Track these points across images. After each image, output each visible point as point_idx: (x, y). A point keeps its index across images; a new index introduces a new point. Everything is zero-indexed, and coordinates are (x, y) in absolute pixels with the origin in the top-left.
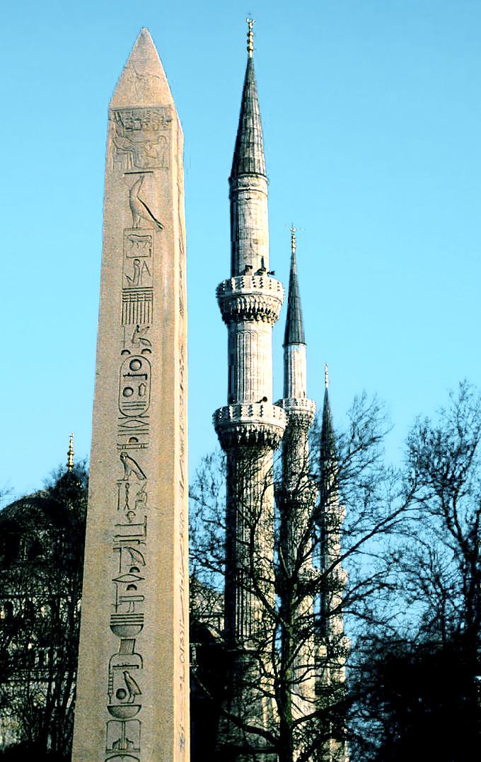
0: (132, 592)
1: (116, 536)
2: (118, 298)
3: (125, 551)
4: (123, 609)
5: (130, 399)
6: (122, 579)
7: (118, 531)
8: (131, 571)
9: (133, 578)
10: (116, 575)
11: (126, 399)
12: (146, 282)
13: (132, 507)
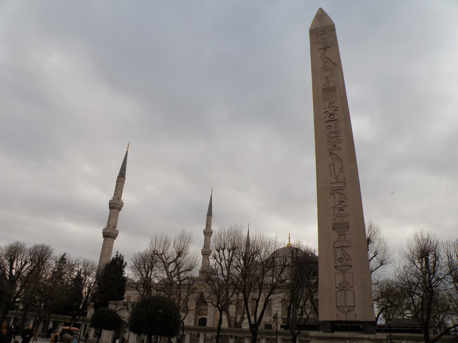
0: (342, 212)
1: (332, 188)
2: (321, 93)
3: (336, 194)
4: (338, 220)
5: (331, 130)
6: (337, 207)
7: (332, 185)
8: (340, 202)
9: (342, 206)
10: (334, 205)
11: (329, 131)
12: (332, 85)
13: (337, 174)
